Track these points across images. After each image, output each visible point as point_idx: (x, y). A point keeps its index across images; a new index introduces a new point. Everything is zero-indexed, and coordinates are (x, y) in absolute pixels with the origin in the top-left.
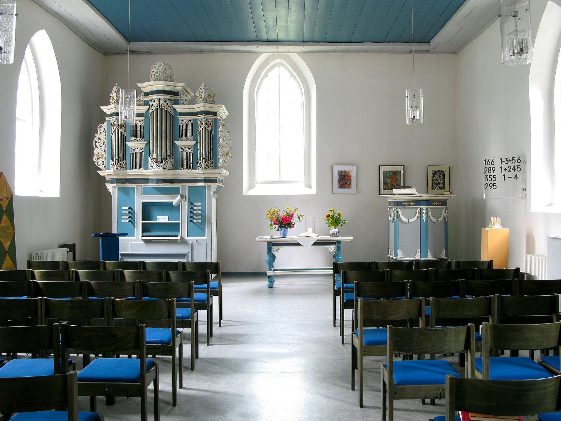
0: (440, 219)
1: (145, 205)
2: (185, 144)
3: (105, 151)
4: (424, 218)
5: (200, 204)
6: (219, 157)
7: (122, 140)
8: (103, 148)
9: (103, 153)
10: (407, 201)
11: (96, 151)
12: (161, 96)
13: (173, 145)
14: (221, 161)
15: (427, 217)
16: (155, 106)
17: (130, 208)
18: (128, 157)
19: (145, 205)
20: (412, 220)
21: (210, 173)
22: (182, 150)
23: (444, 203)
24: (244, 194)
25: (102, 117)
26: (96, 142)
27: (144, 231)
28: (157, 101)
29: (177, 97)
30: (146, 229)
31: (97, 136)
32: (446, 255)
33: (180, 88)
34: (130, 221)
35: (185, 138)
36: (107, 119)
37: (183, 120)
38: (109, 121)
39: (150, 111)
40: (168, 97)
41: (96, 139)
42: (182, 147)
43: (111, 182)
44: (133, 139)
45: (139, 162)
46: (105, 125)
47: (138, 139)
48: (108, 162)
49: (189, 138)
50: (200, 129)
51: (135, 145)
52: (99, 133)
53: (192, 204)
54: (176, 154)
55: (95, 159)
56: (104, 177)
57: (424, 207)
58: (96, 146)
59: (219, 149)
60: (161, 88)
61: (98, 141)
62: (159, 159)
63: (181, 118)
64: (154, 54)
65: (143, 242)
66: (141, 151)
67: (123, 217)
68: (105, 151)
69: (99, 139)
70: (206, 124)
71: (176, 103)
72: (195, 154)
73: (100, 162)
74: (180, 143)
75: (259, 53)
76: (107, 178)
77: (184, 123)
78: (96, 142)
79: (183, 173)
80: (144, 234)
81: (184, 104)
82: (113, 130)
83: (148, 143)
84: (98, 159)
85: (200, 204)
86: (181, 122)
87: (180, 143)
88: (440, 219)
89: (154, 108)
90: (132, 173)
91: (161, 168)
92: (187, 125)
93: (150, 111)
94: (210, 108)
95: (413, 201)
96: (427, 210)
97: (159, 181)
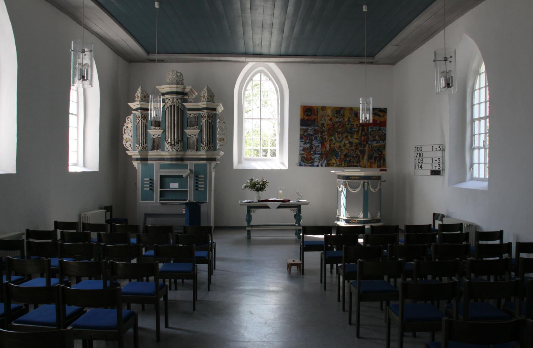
0: (377, 189)
1: (161, 177)
2: (191, 132)
4: (366, 189)
5: (203, 176)
7: (145, 128)
8: (130, 134)
9: (130, 138)
10: (354, 176)
11: (125, 136)
12: (174, 96)
13: (183, 133)
14: (218, 145)
15: (367, 188)
17: (150, 179)
18: (149, 142)
19: (161, 177)
20: (357, 190)
21: (211, 154)
23: (379, 178)
24: (234, 168)
25: (129, 111)
27: (161, 196)
28: (171, 100)
29: (186, 97)
31: (126, 125)
32: (381, 216)
33: (189, 90)
34: (150, 189)
36: (134, 112)
37: (191, 114)
38: (134, 114)
39: (166, 107)
40: (180, 96)
41: (125, 127)
42: (190, 134)
43: (137, 160)
44: (153, 127)
45: (158, 145)
46: (131, 117)
48: (134, 145)
49: (195, 127)
50: (203, 121)
51: (154, 132)
53: (197, 176)
54: (185, 140)
55: (124, 142)
56: (131, 156)
57: (366, 181)
59: (218, 136)
60: (174, 90)
62: (173, 143)
63: (189, 112)
64: (167, 62)
65: (160, 205)
67: (145, 186)
69: (127, 127)
70: (208, 117)
71: (186, 101)
74: (188, 131)
75: (246, 63)
76: (133, 157)
79: (190, 153)
80: (161, 198)
81: (191, 102)
82: (138, 121)
83: (165, 131)
85: (203, 176)
87: (188, 131)
88: (377, 189)
89: (169, 105)
90: (152, 154)
91: (174, 150)
92: (194, 118)
93: (166, 107)
94: (211, 105)
95: (358, 176)
96: (368, 183)
97: (172, 160)
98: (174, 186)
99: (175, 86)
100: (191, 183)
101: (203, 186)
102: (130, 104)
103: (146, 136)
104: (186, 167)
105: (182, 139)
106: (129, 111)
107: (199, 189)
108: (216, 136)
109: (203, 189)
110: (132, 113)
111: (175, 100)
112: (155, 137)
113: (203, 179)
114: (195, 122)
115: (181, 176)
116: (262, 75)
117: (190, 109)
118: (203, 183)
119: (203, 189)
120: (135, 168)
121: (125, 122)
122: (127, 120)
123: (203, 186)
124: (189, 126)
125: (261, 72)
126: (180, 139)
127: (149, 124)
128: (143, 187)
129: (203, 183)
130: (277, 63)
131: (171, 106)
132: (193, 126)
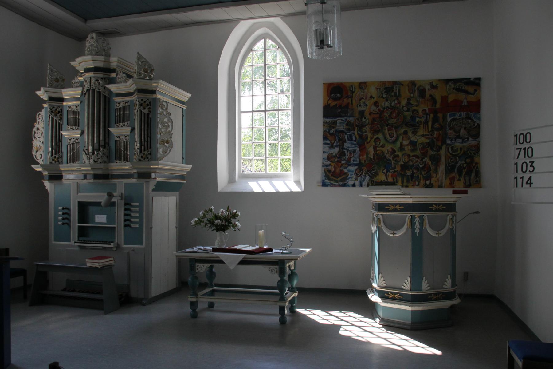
0: (443, 232)
2: (119, 131)
3: (43, 143)
4: (417, 230)
5: (137, 204)
6: (158, 145)
8: (42, 140)
9: (42, 145)
10: (393, 204)
12: (91, 74)
13: (107, 134)
14: (161, 150)
15: (421, 229)
16: (87, 86)
18: (64, 150)
20: (399, 234)
21: (143, 166)
22: (118, 139)
23: (450, 207)
24: (220, 189)
26: (35, 132)
29: (113, 75)
30: (83, 233)
31: (36, 125)
32: (453, 284)
33: (115, 64)
35: (121, 124)
40: (100, 75)
41: (35, 129)
42: (118, 134)
44: (70, 127)
47: (74, 127)
49: (126, 123)
52: (37, 122)
55: (34, 153)
57: (417, 214)
58: (35, 137)
59: (159, 136)
61: (37, 132)
63: (116, 99)
64: (125, 34)
65: (78, 249)
66: (77, 141)
68: (43, 143)
69: (38, 129)
70: (141, 105)
71: (112, 81)
73: (38, 155)
74: (115, 131)
75: (234, 22)
77: (120, 106)
78: (35, 132)
79: (117, 167)
80: (81, 239)
81: (120, 82)
84: (37, 152)
85: (137, 204)
86: (117, 105)
87: (115, 131)
88: (443, 232)
91: (92, 161)
94: (145, 84)
95: (401, 205)
96: (421, 218)
98: (101, 219)
103: (60, 140)
109: (137, 226)
110: (43, 107)
111: (93, 81)
116: (268, 40)
117: (118, 95)
119: (137, 226)
120: (47, 190)
121: (36, 122)
122: (37, 118)
124: (117, 122)
125: (264, 36)
126: (102, 143)
128: (56, 220)
130: (284, 17)
132: (124, 121)
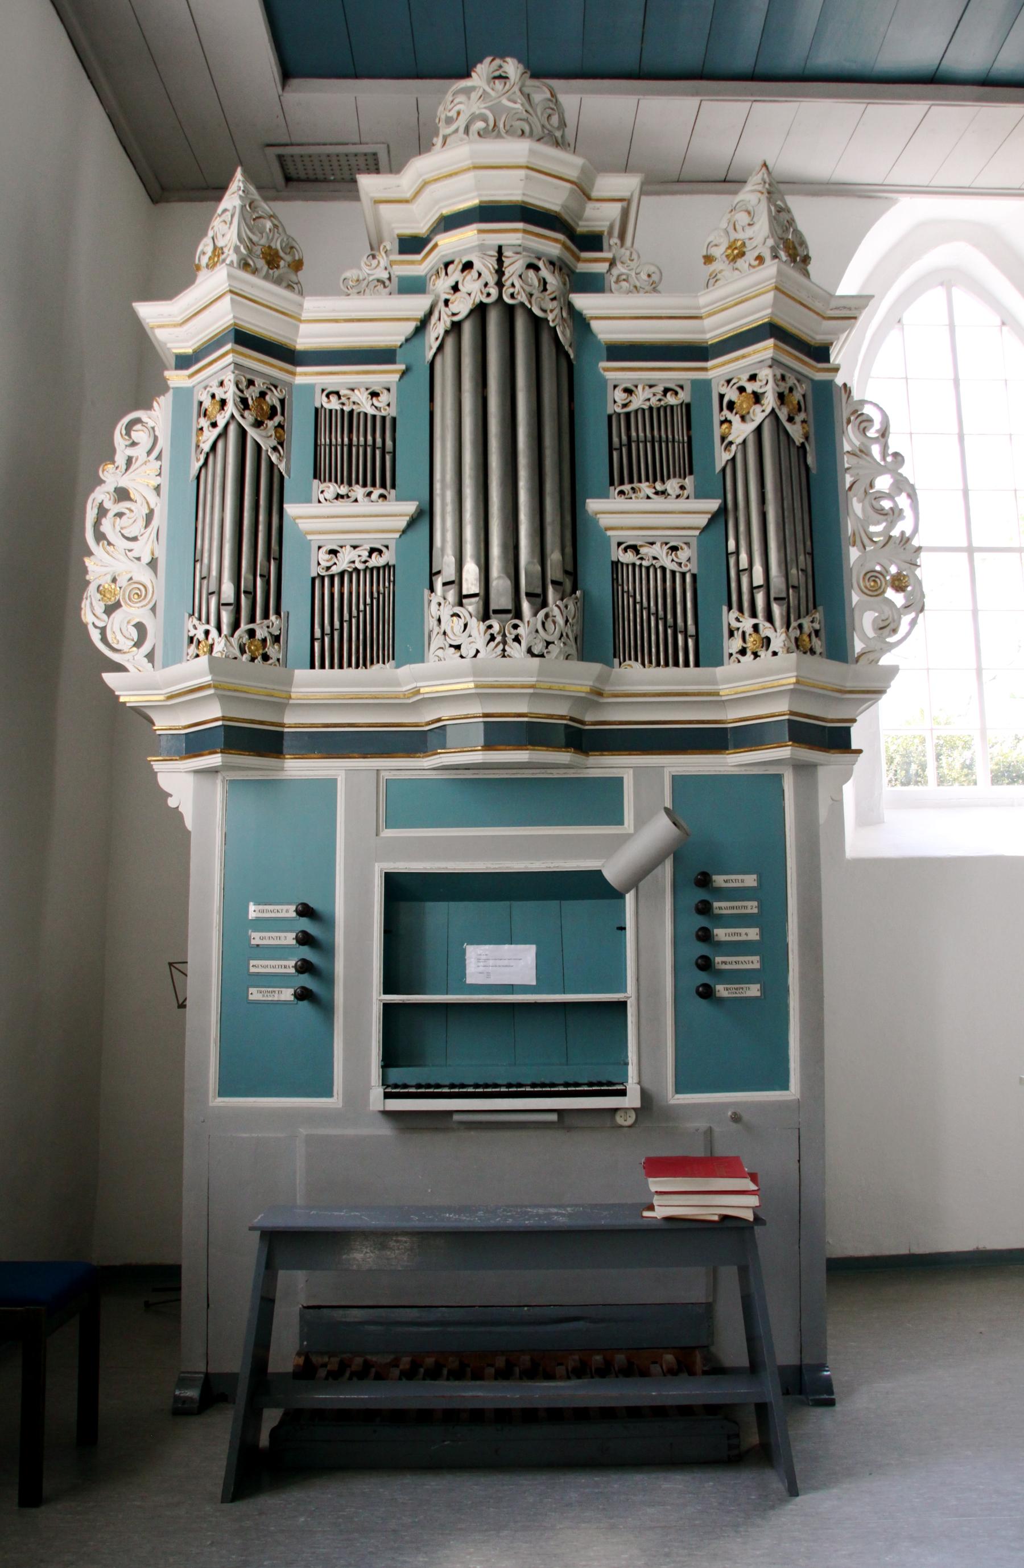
1: (401, 892)
2: (645, 521)
3: (153, 564)
5: (750, 880)
6: (855, 598)
7: (262, 495)
8: (144, 549)
9: (145, 576)
11: (101, 565)
12: (512, 235)
16: (474, 290)
17: (306, 911)
19: (401, 892)
22: (629, 557)
25: (142, 373)
26: (102, 511)
27: (392, 1056)
28: (485, 265)
30: (402, 1038)
31: (111, 477)
34: (303, 995)
35: (645, 488)
36: (176, 378)
37: (630, 388)
38: (183, 395)
39: (437, 329)
40: (552, 245)
41: (101, 495)
42: (631, 537)
43: (195, 743)
44: (331, 489)
46: (159, 416)
47: (359, 491)
48: (171, 627)
49: (672, 485)
50: (741, 431)
51: (334, 524)
52: (120, 459)
53: (704, 881)
54: (597, 582)
55: (91, 612)
56: (141, 715)
58: (100, 537)
59: (854, 554)
60: (509, 189)
61: (113, 508)
62: (501, 598)
63: (616, 374)
65: (385, 1130)
66: (376, 561)
67: (258, 966)
68: (153, 564)
69: (122, 494)
70: (781, 397)
71: (593, 284)
72: (717, 582)
73: (120, 629)
76: (162, 723)
77: (638, 402)
78: (102, 511)
79: (645, 689)
80: (397, 1074)
82: (210, 435)
83: (425, 515)
84: (110, 610)
85: (750, 880)
86: (620, 396)
89: (462, 306)
90: (319, 693)
91: (517, 651)
92: (655, 414)
93: (437, 329)
97: (499, 733)
99: (519, 149)
100: (649, 942)
101: (752, 962)
102: (147, 311)
103: (276, 555)
104: (602, 802)
105: (572, 577)
106: (142, 373)
107: (722, 990)
108: (837, 559)
109: (753, 990)
110: (163, 388)
111: (514, 267)
112: (342, 564)
113: (751, 907)
114: (663, 446)
115: (590, 887)
116: (959, 294)
117: (621, 352)
118: (752, 934)
119: (753, 990)
120: (176, 814)
121: (109, 455)
122: (119, 440)
123: (752, 962)
124: (623, 475)
125: (947, 278)
126: (554, 571)
127: (296, 463)
128: (236, 979)
129: (752, 934)
131: (480, 310)
132: (656, 475)
